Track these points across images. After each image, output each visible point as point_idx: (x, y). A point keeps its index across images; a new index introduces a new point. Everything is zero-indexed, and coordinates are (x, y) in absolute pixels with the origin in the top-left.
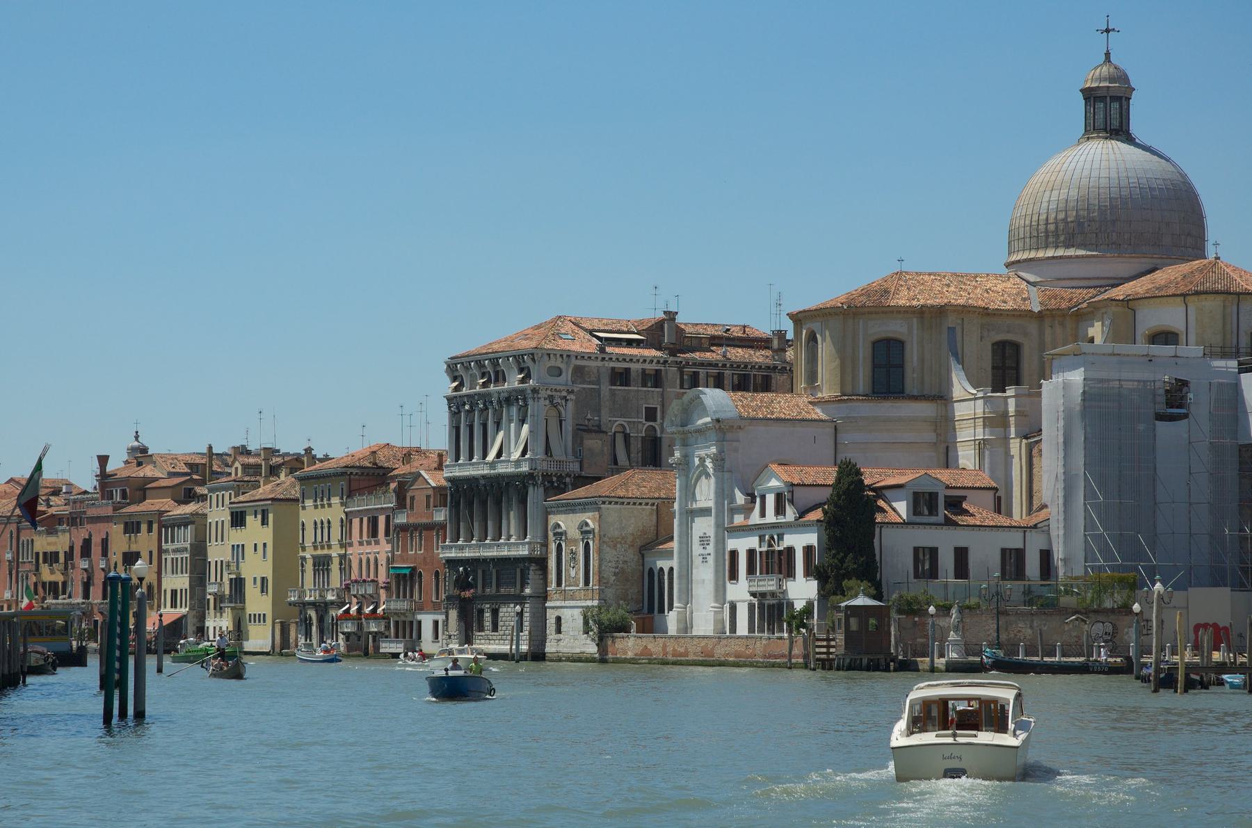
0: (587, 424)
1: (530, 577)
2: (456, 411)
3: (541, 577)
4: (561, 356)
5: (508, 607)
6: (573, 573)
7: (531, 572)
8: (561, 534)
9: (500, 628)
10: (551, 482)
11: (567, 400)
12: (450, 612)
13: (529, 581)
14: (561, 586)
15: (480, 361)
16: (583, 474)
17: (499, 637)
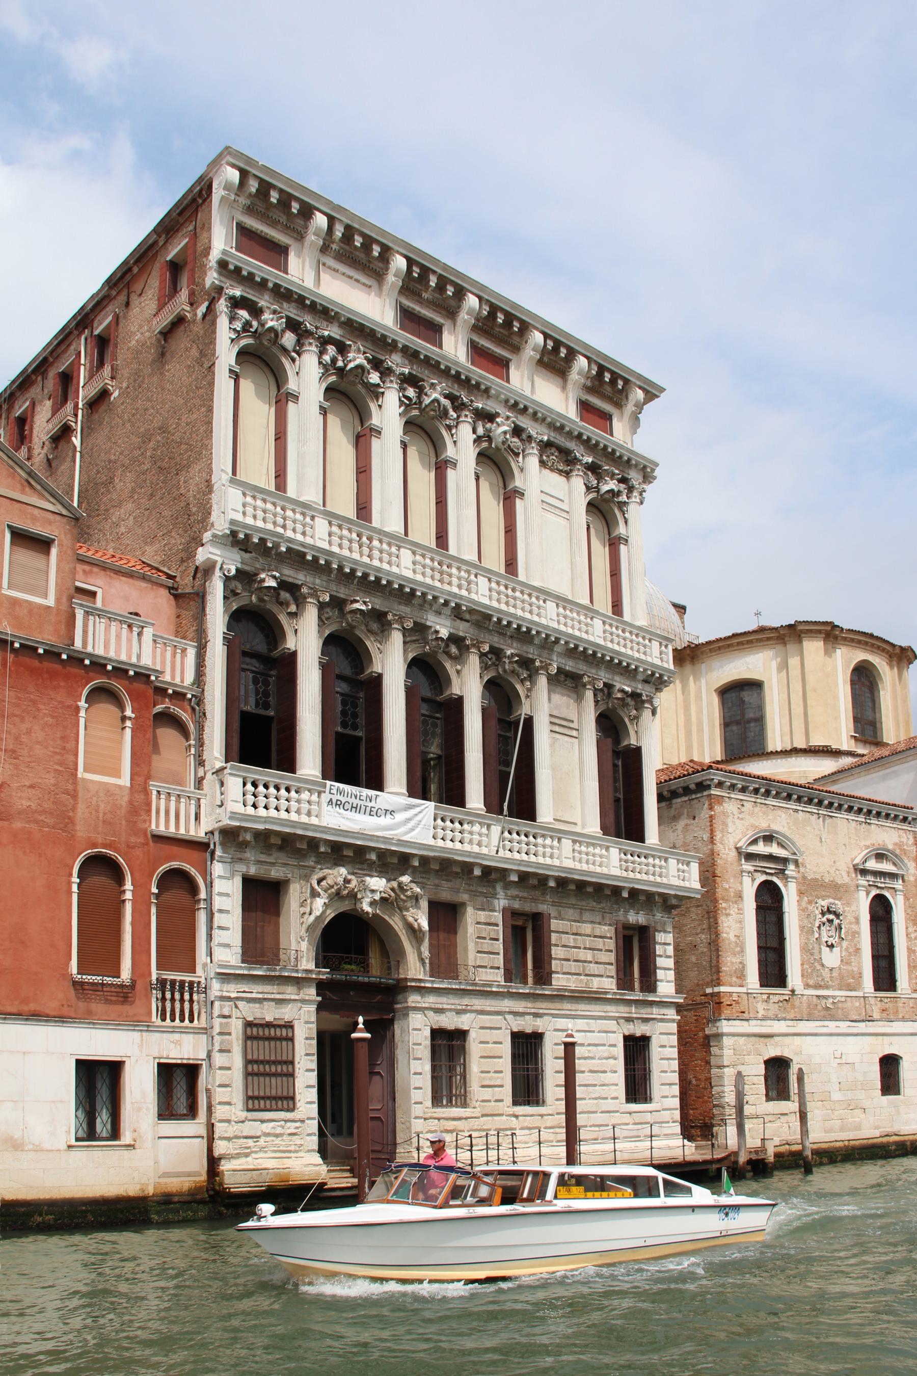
6: (831, 959)
8: (785, 861)
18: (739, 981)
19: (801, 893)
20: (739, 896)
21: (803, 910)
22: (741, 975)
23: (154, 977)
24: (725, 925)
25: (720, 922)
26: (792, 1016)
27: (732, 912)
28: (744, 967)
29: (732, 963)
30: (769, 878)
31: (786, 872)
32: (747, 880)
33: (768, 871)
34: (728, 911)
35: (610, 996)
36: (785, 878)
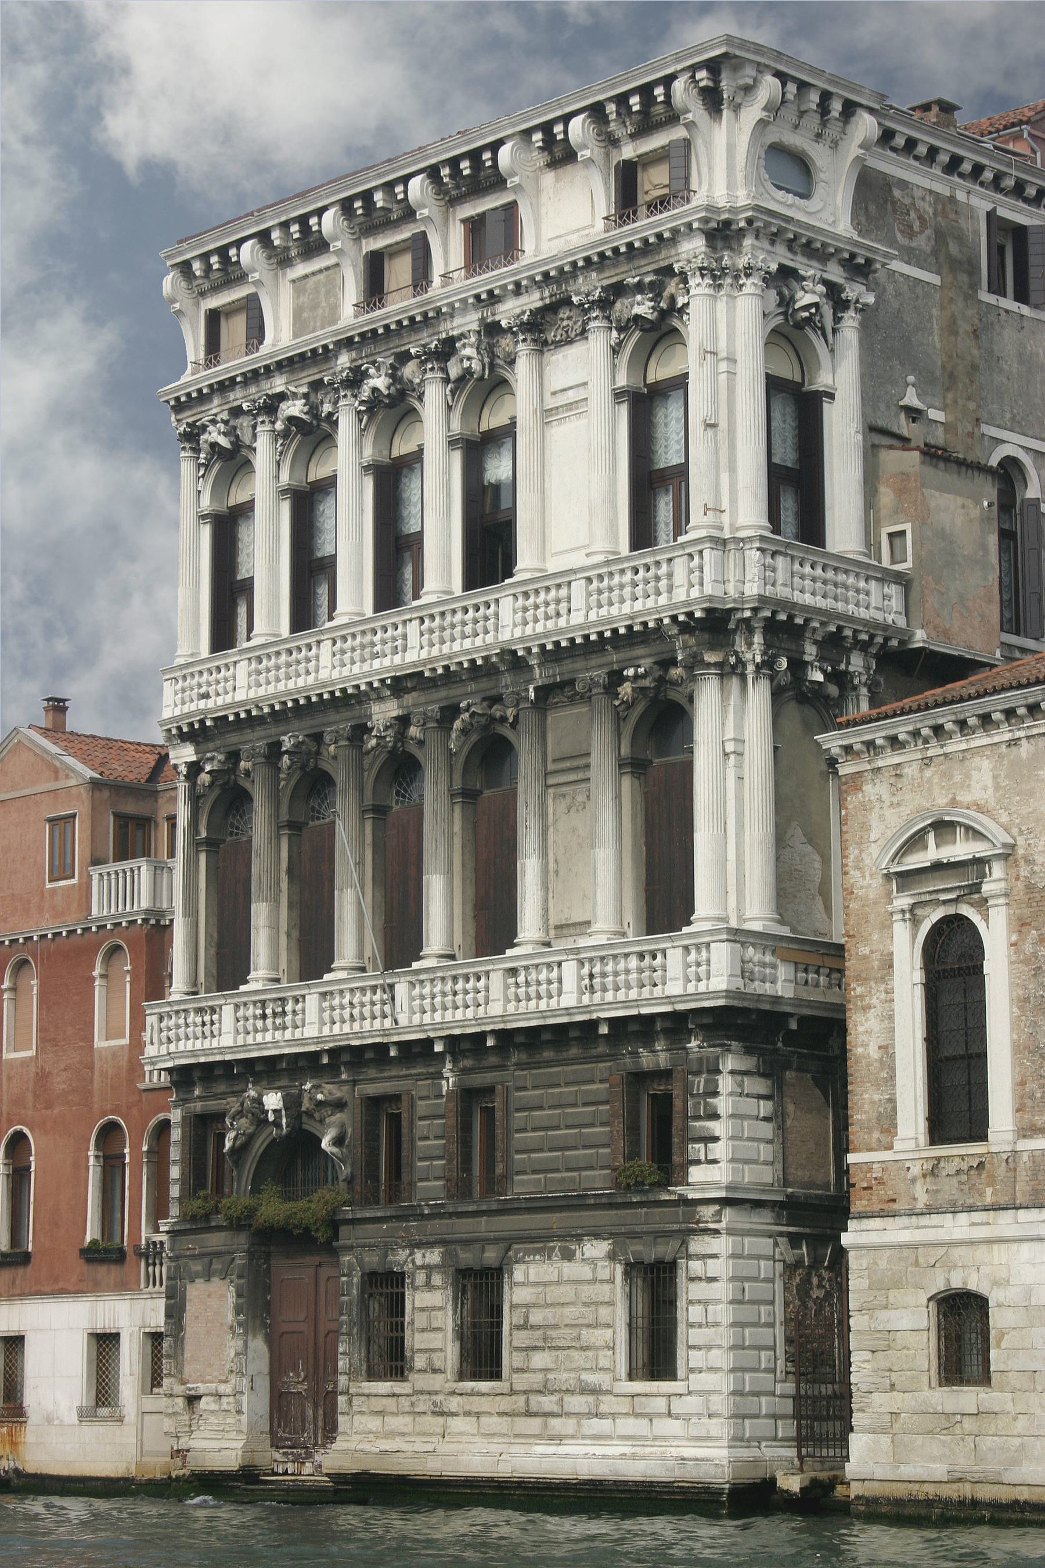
0: (905, 433)
1: (723, 1104)
2: (224, 442)
3: (765, 1108)
4: (826, 97)
5: (568, 1256)
7: (725, 1083)
9: (509, 1359)
10: (798, 666)
11: (840, 305)
12: (196, 1292)
13: (717, 1127)
14: (982, 1136)
15: (367, 196)
16: (920, 638)
17: (505, 1404)
18: (885, 1139)
19: (1021, 925)
20: (888, 964)
21: (1026, 962)
22: (888, 1124)
23: (143, 1242)
24: (860, 1029)
25: (850, 1025)
26: (989, 1199)
27: (874, 1001)
28: (894, 1109)
29: (872, 1102)
30: (951, 910)
31: (985, 888)
32: (901, 931)
33: (944, 897)
34: (867, 1000)
35: (592, 1201)
36: (982, 905)
